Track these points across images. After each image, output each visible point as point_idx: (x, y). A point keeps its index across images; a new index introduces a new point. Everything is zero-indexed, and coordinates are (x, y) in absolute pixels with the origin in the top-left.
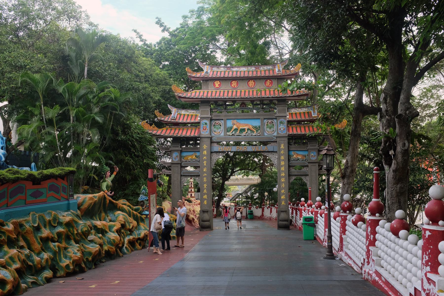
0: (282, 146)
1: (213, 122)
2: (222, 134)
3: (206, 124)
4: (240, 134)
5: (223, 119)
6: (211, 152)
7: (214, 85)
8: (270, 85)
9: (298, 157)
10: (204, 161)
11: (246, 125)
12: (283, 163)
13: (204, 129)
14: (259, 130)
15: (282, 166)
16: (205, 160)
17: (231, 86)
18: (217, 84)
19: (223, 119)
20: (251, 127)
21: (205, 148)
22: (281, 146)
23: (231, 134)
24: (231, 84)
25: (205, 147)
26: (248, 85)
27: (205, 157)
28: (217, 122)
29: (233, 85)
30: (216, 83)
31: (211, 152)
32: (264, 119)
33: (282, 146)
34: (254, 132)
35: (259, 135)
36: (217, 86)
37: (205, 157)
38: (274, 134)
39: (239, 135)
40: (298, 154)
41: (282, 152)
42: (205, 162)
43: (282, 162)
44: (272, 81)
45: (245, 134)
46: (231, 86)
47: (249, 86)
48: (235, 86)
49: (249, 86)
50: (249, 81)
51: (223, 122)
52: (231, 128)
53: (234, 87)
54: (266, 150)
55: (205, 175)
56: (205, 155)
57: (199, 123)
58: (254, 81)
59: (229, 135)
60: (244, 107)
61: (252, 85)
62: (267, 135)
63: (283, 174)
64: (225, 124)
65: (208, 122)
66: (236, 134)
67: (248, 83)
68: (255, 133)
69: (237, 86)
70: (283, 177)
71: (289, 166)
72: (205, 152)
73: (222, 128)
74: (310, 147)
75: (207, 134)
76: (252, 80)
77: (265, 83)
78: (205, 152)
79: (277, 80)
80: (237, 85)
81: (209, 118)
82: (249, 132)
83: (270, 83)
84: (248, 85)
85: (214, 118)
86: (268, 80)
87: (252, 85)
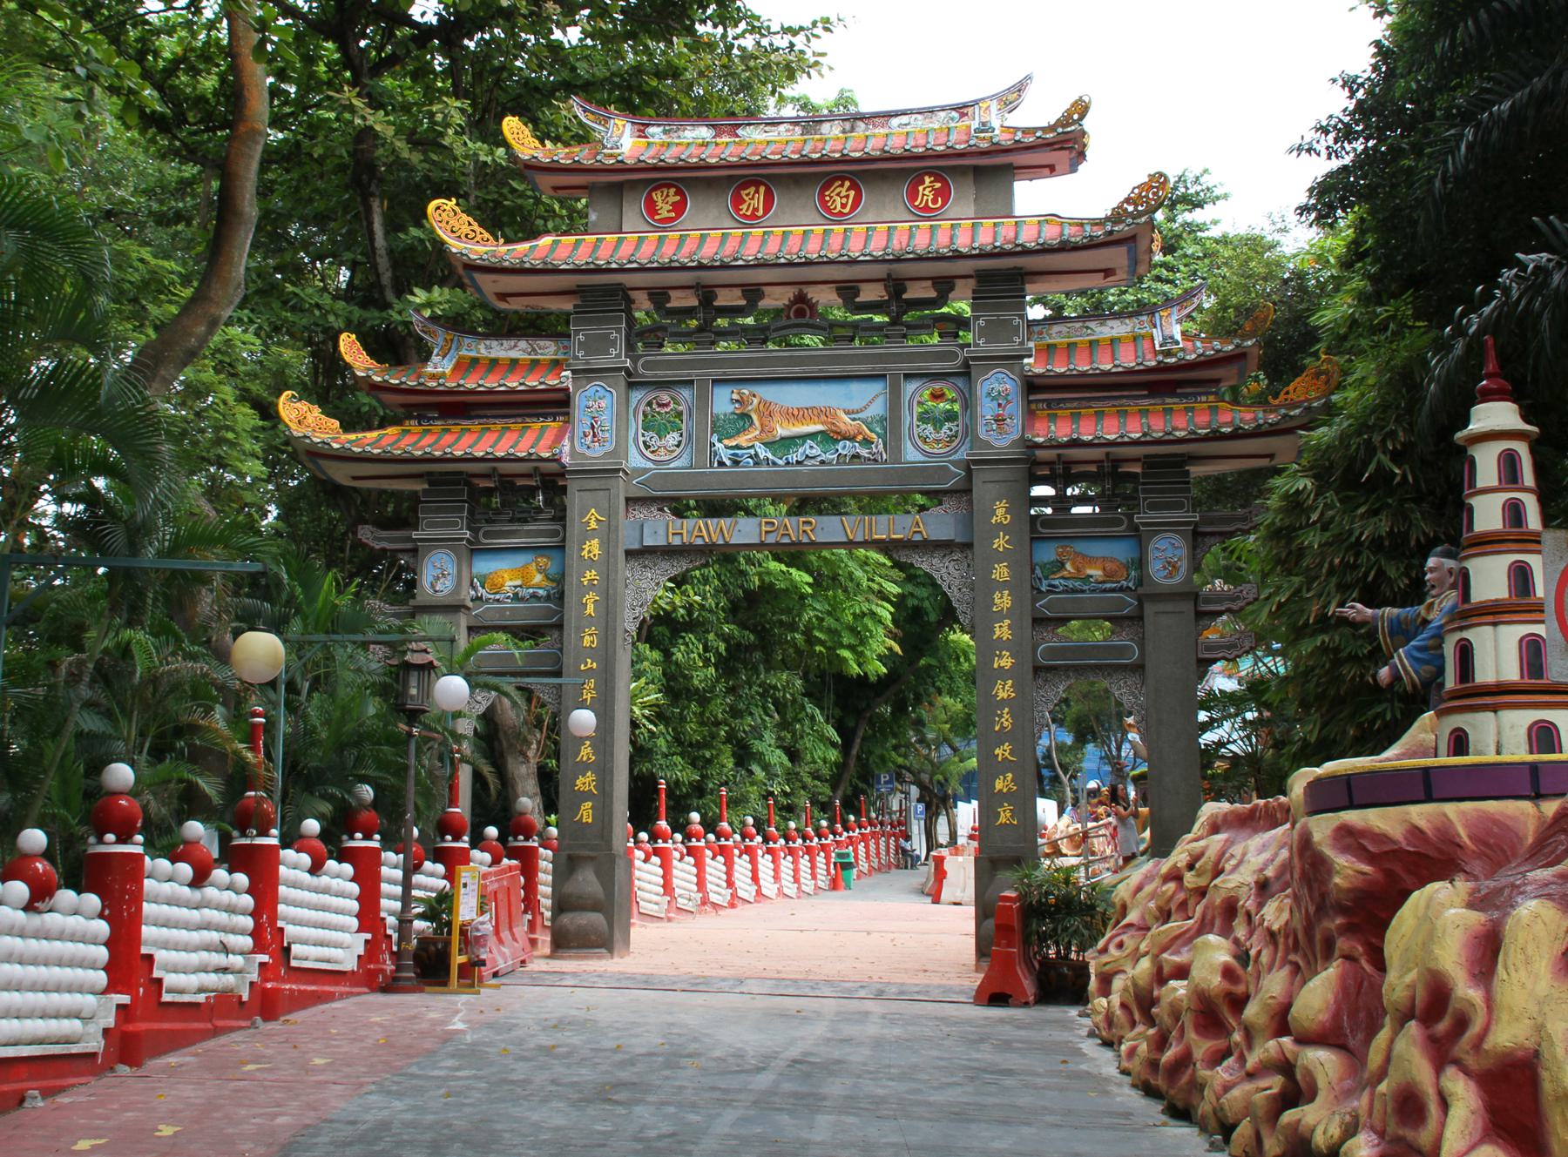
7: (652, 208)
8: (935, 201)
9: (1090, 572)
10: (583, 590)
12: (1003, 600)
15: (1000, 616)
16: (592, 586)
17: (737, 210)
18: (664, 202)
19: (692, 382)
21: (593, 525)
22: (993, 513)
24: (738, 201)
25: (593, 518)
26: (824, 203)
27: (590, 574)
29: (744, 207)
30: (657, 196)
32: (908, 377)
33: (1001, 514)
36: (664, 211)
37: (590, 574)
40: (1084, 556)
41: (1000, 543)
43: (997, 595)
44: (946, 185)
46: (737, 210)
47: (828, 210)
48: (756, 210)
49: (828, 210)
50: (827, 186)
53: (754, 216)
54: (918, 538)
55: (591, 664)
58: (854, 186)
60: (806, 320)
62: (921, 458)
63: (1006, 662)
67: (822, 195)
69: (767, 211)
70: (1002, 674)
71: (1039, 621)
72: (593, 548)
74: (1152, 514)
76: (843, 179)
77: (913, 195)
78: (593, 548)
79: (971, 177)
80: (767, 209)
81: (619, 369)
83: (937, 193)
84: (824, 203)
86: (927, 180)
87: (843, 206)
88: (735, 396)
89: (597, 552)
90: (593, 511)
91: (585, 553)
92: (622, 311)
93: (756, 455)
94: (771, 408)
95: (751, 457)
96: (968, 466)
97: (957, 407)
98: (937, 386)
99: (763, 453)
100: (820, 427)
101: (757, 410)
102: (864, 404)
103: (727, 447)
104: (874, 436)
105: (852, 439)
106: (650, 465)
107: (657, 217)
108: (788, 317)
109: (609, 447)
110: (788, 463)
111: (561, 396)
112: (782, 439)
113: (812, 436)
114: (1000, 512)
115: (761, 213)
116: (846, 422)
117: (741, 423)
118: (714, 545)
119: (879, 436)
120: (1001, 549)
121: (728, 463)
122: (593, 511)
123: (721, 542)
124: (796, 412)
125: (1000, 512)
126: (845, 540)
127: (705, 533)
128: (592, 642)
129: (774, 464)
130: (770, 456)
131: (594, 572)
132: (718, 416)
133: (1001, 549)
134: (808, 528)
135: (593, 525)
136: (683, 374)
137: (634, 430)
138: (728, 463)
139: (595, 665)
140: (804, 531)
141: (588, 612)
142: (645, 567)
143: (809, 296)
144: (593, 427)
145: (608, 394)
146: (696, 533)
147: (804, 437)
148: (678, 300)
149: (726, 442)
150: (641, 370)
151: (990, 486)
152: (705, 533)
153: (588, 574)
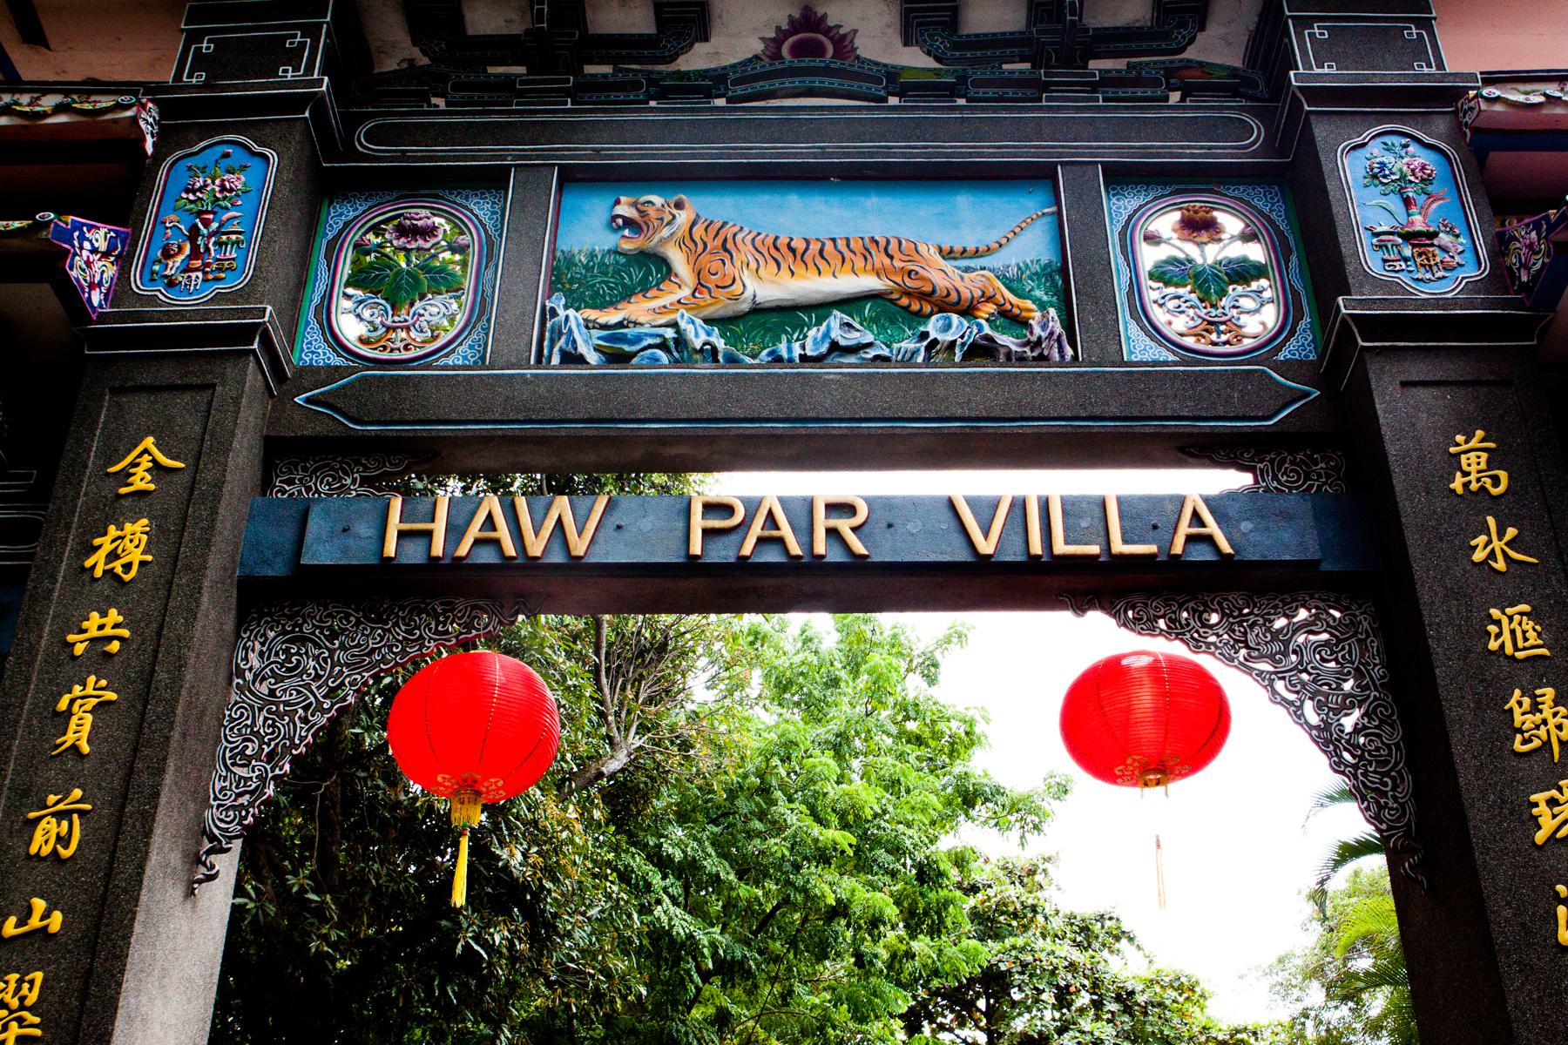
43: (1517, 702)
88: (624, 210)
90: (149, 442)
91: (100, 557)
93: (681, 341)
94: (729, 231)
95: (663, 346)
97: (1256, 252)
98: (1197, 201)
99: (698, 336)
100: (870, 283)
101: (688, 241)
102: (991, 238)
103: (589, 325)
104: (1029, 304)
105: (968, 311)
108: (777, 56)
110: (778, 359)
112: (758, 310)
113: (849, 303)
116: (943, 276)
117: (637, 275)
118: (533, 565)
119: (1043, 306)
120: (1500, 565)
121: (593, 358)
122: (149, 442)
123: (557, 558)
124: (799, 245)
126: (963, 555)
127: (503, 532)
128: (64, 840)
129: (732, 360)
130: (720, 344)
131: (114, 616)
132: (570, 261)
133: (1500, 565)
134: (844, 525)
135: (141, 480)
136: (483, 155)
137: (321, 287)
138: (593, 358)
139: (56, 921)
140: (832, 532)
141: (70, 738)
142: (302, 640)
143: (831, 22)
144: (194, 232)
145: (255, 163)
147: (820, 308)
149: (592, 314)
150: (362, 144)
151: (1423, 394)
152: (503, 532)
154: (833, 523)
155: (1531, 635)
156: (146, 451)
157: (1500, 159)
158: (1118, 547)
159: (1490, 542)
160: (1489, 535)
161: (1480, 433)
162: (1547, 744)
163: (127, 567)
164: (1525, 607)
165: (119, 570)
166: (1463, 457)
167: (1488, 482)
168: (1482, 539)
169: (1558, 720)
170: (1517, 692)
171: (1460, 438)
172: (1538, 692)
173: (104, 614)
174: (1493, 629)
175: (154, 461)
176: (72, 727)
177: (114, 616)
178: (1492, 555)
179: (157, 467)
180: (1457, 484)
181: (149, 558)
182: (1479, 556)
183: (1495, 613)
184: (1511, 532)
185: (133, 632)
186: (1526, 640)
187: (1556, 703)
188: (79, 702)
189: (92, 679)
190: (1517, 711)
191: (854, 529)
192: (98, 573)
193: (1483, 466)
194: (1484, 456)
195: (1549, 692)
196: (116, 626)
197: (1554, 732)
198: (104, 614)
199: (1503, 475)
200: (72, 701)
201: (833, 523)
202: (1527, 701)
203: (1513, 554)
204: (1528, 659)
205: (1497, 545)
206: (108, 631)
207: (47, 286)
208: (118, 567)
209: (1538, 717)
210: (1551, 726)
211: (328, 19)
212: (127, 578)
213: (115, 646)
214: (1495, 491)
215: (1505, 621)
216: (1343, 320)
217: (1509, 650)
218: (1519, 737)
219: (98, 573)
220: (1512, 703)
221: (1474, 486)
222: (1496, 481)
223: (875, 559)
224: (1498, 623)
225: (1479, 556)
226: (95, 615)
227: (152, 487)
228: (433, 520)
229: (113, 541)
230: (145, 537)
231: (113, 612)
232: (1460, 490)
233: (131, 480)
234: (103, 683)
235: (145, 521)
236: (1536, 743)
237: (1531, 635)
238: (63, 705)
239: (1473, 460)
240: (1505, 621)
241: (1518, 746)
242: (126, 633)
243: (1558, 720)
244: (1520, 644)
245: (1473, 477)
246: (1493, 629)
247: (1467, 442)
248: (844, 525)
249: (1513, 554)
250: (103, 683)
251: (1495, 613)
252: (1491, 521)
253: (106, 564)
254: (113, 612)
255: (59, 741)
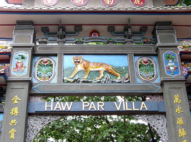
0: (177, 99)
1: (38, 60)
2: (55, 81)
3: (23, 58)
4: (90, 81)
5: (56, 55)
6: (29, 115)
8: (140, 3)
11: (102, 65)
13: (17, 66)
14: (125, 73)
16: (13, 126)
20: (110, 68)
21: (16, 102)
22: (174, 99)
23: (72, 80)
28: (45, 59)
31: (29, 115)
32: (135, 55)
34: (117, 76)
35: (127, 81)
38: (156, 82)
39: (88, 82)
41: (178, 110)
42: (13, 131)
43: (180, 130)
45: (99, 81)
51: (56, 59)
52: (71, 70)
56: (14, 117)
57: (9, 54)
59: (68, 82)
61: (111, 2)
64: (61, 62)
65: (27, 55)
66: (82, 80)
68: (119, 78)
72: (15, 111)
73: (55, 69)
75: (23, 76)
78: (15, 111)
82: (108, 76)
85: (38, 51)
89: (17, 112)
90: (16, 96)
91: (12, 112)
92: (33, 29)
96: (162, 84)
106: (38, 82)
107: (47, 3)
109: (24, 74)
111: (7, 56)
114: (177, 99)
115: (82, 3)
125: (177, 99)
133: (179, 112)
134: (101, 106)
141: (11, 137)
146: (56, 107)
148: (52, 29)
153: (12, 121)
154: (100, 106)
155: (182, 122)
156: (16, 98)
157: (182, 55)
158: (134, 109)
159: (178, 110)
160: (178, 108)
161: (178, 95)
162: (183, 135)
163: (16, 114)
164: (181, 118)
165: (15, 114)
166: (176, 98)
167: (178, 102)
168: (177, 109)
169: (184, 133)
170: (180, 129)
171: (175, 96)
172: (182, 129)
173: (13, 120)
174: (178, 121)
175: (17, 99)
176: (12, 136)
177: (15, 120)
178: (178, 111)
179: (17, 100)
180: (175, 102)
181: (18, 112)
182: (177, 111)
183: (178, 119)
184: (180, 108)
185: (18, 122)
186: (181, 122)
187: (184, 130)
188: (12, 132)
189: (13, 129)
190: (180, 132)
191: (102, 107)
192: (12, 114)
193: (178, 99)
194: (178, 98)
195: (183, 129)
196: (15, 122)
197: (184, 134)
198: (13, 120)
199: (180, 101)
200: (11, 132)
201: (100, 106)
202: (181, 130)
203: (181, 111)
204: (181, 125)
205: (179, 110)
206: (14, 122)
207: (3, 77)
208: (14, 113)
209: (182, 132)
210: (183, 133)
211: (33, 33)
212: (16, 115)
213: (15, 124)
214: (179, 103)
215: (179, 120)
216: (162, 81)
217: (179, 124)
218: (180, 135)
219: (12, 114)
220: (179, 131)
221: (176, 102)
222: (179, 101)
223: (105, 111)
224: (178, 120)
225: (177, 111)
226: (12, 120)
227: (17, 103)
228: (51, 105)
229: (14, 110)
230: (17, 110)
231: (15, 120)
232: (175, 103)
233: (15, 102)
234: (14, 129)
235: (17, 107)
236: (182, 136)
237: (182, 122)
238: (10, 133)
239: (177, 98)
240: (179, 120)
241: (180, 136)
242: (16, 123)
243: (184, 133)
244: (181, 123)
245: (177, 101)
246: (178, 121)
247: (176, 96)
248: (101, 106)
249: (181, 111)
250: (14, 129)
251: (178, 119)
252: (178, 107)
253: (13, 113)
254: (15, 120)
255: (10, 137)
